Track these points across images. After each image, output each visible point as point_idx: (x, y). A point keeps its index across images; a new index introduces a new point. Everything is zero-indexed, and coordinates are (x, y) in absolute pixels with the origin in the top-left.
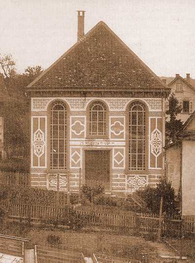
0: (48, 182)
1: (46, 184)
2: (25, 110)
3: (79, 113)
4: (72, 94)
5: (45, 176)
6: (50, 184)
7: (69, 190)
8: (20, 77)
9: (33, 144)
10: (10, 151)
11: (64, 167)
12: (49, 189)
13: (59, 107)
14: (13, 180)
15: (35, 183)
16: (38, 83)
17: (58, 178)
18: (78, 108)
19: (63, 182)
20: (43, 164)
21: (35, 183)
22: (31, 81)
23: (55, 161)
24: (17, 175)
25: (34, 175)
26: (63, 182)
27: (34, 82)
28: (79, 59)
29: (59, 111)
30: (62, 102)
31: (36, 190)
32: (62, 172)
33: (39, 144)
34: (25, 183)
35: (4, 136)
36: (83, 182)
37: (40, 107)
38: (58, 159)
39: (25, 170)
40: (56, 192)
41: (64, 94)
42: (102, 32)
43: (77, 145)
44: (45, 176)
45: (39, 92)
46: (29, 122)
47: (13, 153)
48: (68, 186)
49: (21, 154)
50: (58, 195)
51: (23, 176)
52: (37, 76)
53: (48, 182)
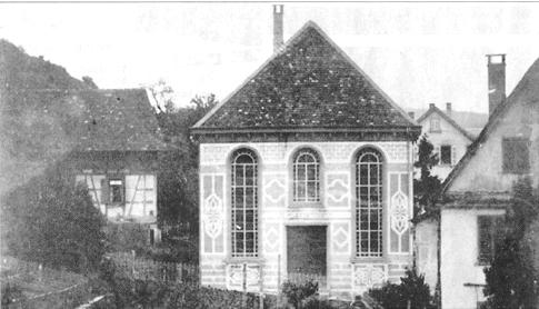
0: (228, 278)
1: (224, 280)
2: (194, 161)
3: (277, 167)
4: (264, 137)
5: (223, 267)
6: (232, 281)
7: (261, 290)
8: (181, 112)
9: (203, 217)
10: (167, 228)
11: (254, 253)
12: (230, 288)
13: (247, 159)
14: (172, 274)
15: (208, 279)
16: (210, 122)
17: (244, 270)
18: (274, 158)
19: (252, 276)
20: (220, 249)
21: (208, 279)
22: (200, 117)
23: (240, 245)
24: (179, 267)
25: (206, 267)
26: (252, 276)
27: (202, 121)
28: (276, 81)
29: (245, 163)
30: (250, 150)
31: (208, 290)
32: (249, 262)
33: (215, 217)
34: (196, 278)
35: (158, 205)
36: (284, 277)
37: (215, 158)
38: (245, 239)
39: (192, 258)
40: (241, 293)
41: (251, 137)
42: (312, 38)
43: (276, 218)
44: (223, 267)
45: (214, 135)
46: (197, 181)
47: (174, 232)
48: (260, 283)
49: (184, 232)
50: (245, 298)
51: (190, 270)
52: (208, 109)
53: (228, 278)
